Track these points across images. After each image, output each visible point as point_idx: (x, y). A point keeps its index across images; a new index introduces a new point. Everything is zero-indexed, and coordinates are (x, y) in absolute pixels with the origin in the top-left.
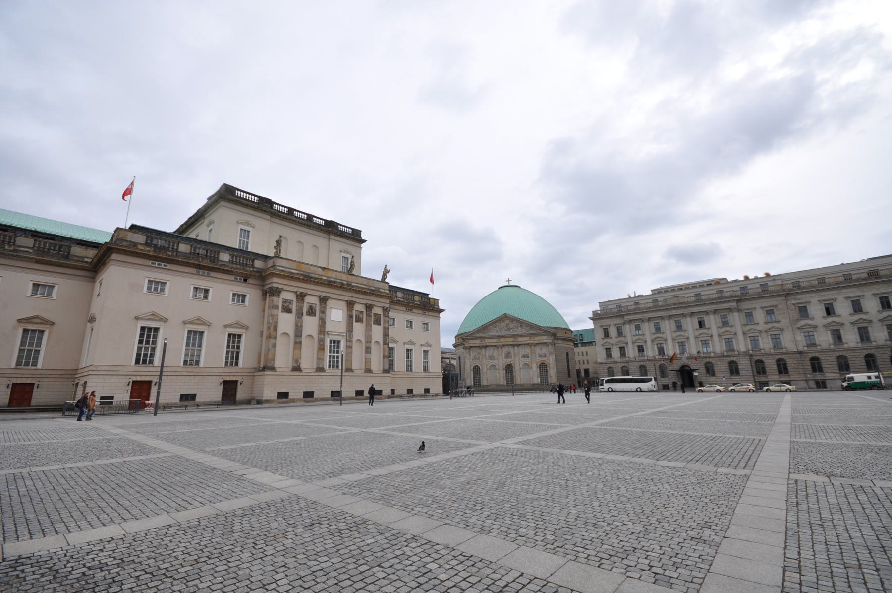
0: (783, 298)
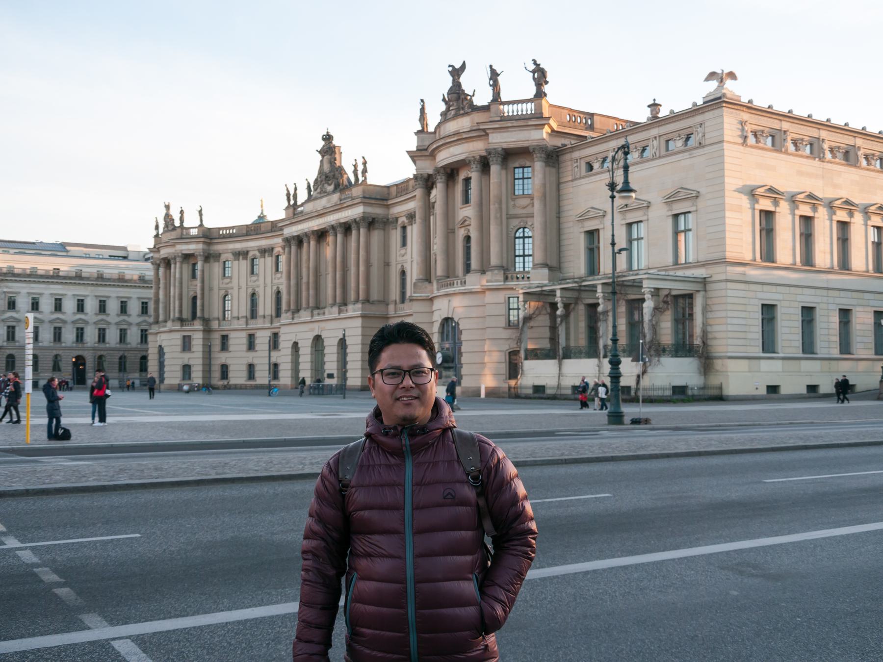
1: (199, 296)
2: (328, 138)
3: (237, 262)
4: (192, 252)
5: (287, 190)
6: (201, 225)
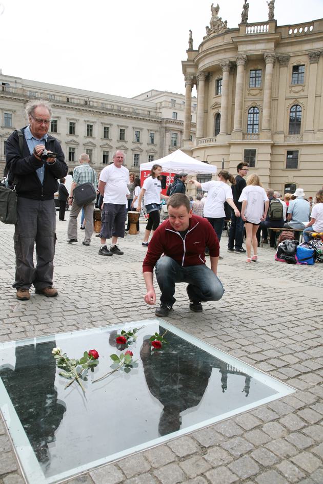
6: (272, 20)
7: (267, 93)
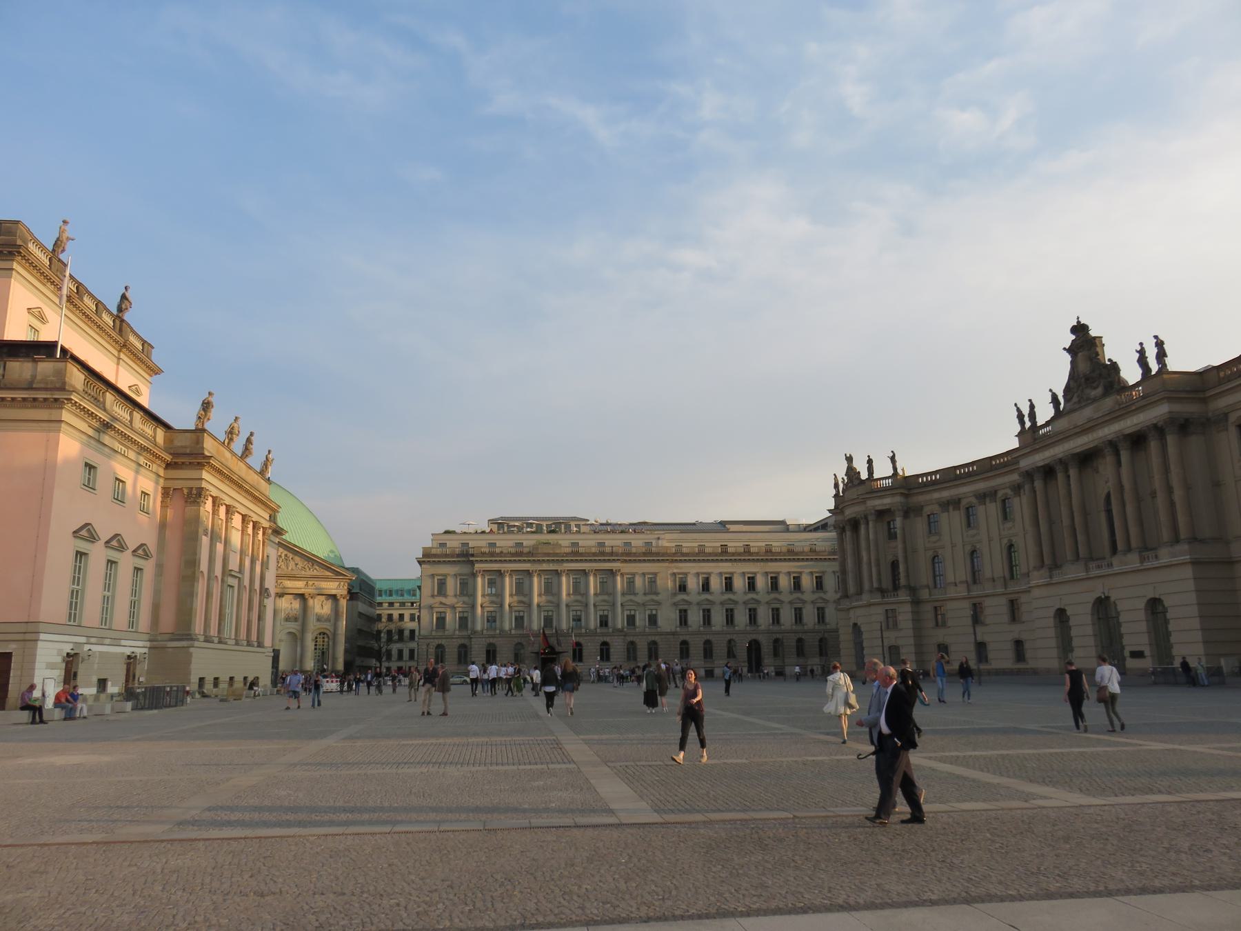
0: (666, 564)
1: (901, 559)
2: (1080, 329)
3: (946, 514)
4: (888, 507)
5: (1018, 410)
7: (900, 546)
